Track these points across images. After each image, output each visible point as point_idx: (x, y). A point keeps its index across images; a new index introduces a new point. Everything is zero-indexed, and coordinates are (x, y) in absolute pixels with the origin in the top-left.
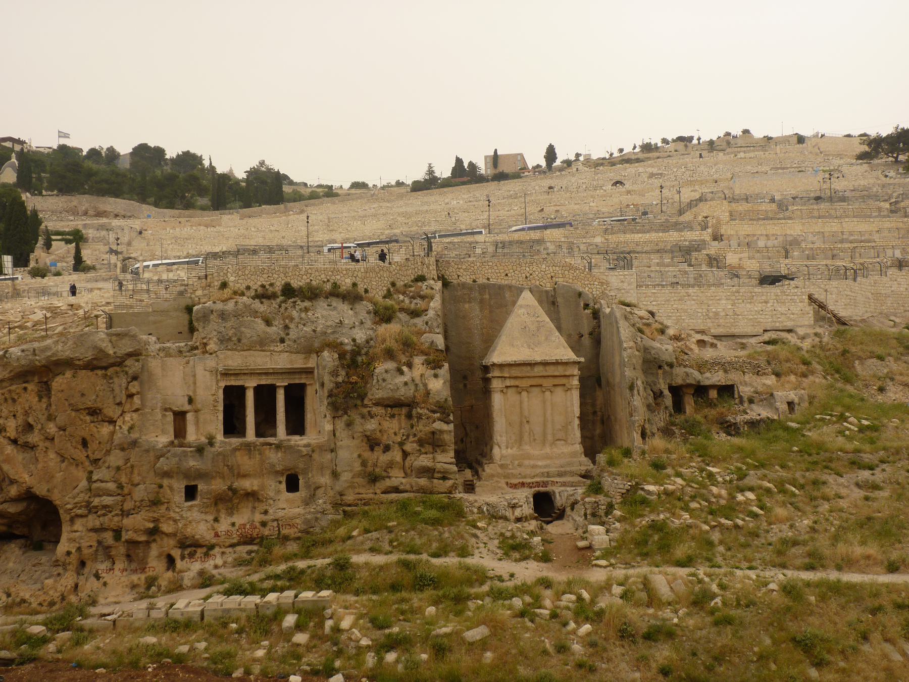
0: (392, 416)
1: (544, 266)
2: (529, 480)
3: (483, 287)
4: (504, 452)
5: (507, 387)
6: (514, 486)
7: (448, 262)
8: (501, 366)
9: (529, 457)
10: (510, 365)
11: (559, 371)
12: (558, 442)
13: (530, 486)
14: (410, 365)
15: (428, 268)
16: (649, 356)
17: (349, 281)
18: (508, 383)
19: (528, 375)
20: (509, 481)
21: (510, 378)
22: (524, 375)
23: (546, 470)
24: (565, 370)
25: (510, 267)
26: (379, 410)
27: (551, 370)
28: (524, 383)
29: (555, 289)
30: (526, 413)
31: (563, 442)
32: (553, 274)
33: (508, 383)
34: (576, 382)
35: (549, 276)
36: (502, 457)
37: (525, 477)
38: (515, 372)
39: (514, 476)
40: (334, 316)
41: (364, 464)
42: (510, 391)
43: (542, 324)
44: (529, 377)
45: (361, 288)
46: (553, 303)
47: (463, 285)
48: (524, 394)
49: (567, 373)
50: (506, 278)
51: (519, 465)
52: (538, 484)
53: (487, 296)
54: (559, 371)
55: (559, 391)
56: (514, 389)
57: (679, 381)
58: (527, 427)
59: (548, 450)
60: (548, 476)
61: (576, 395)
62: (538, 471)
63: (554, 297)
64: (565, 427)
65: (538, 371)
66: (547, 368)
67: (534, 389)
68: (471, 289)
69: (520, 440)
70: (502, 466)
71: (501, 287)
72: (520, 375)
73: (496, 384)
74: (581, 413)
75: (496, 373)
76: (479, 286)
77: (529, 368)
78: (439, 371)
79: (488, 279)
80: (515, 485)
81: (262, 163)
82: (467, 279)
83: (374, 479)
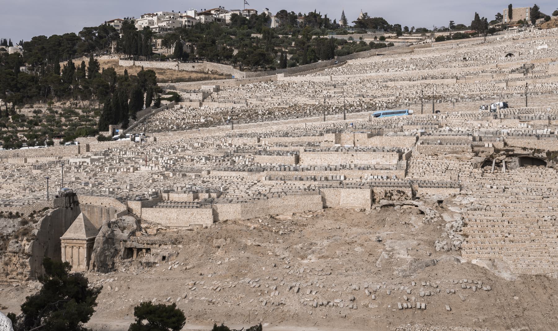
0: (15, 256)
3: (89, 206)
14: (22, 240)
17: (15, 211)
26: (11, 254)
38: (68, 241)
40: (5, 223)
41: (4, 270)
45: (20, 213)
57: (129, 246)
61: (85, 250)
65: (75, 241)
71: (94, 207)
78: (30, 243)
81: (365, 15)
83: (7, 274)
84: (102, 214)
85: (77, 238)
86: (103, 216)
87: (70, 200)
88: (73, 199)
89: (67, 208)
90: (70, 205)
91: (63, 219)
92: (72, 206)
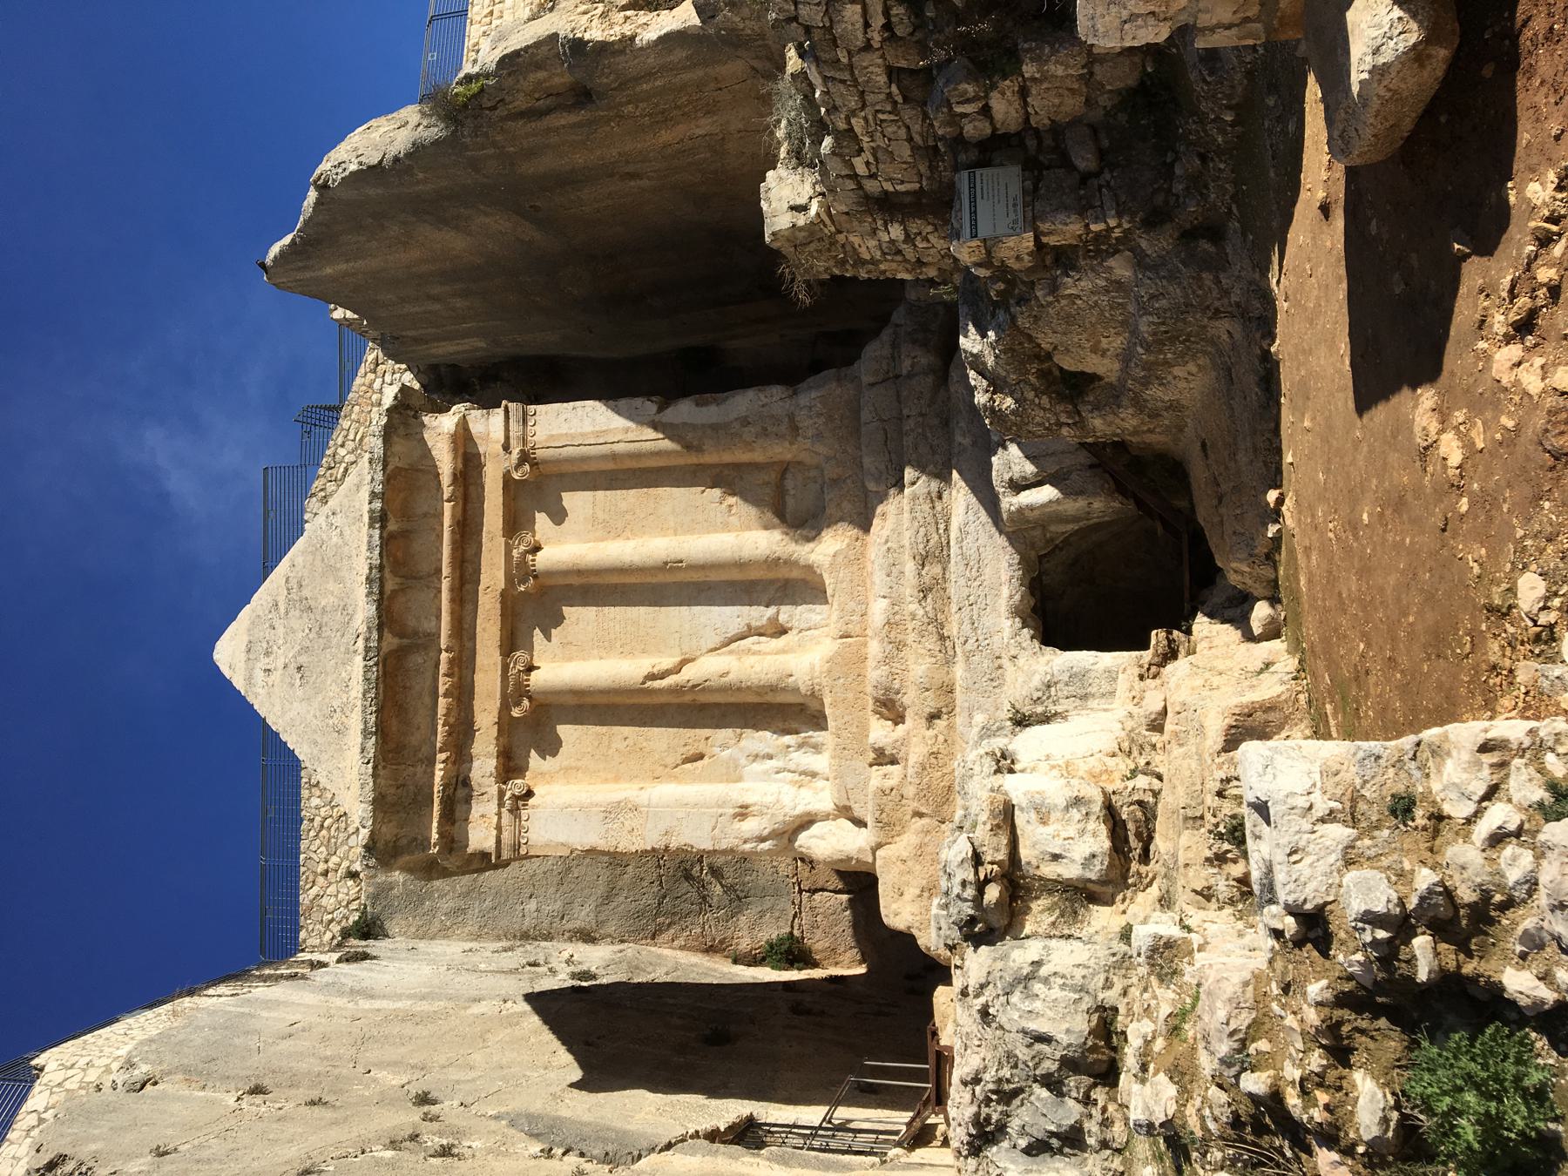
9: (849, 663)
18: (484, 765)
33: (484, 765)
49: (445, 463)
74: (648, 394)
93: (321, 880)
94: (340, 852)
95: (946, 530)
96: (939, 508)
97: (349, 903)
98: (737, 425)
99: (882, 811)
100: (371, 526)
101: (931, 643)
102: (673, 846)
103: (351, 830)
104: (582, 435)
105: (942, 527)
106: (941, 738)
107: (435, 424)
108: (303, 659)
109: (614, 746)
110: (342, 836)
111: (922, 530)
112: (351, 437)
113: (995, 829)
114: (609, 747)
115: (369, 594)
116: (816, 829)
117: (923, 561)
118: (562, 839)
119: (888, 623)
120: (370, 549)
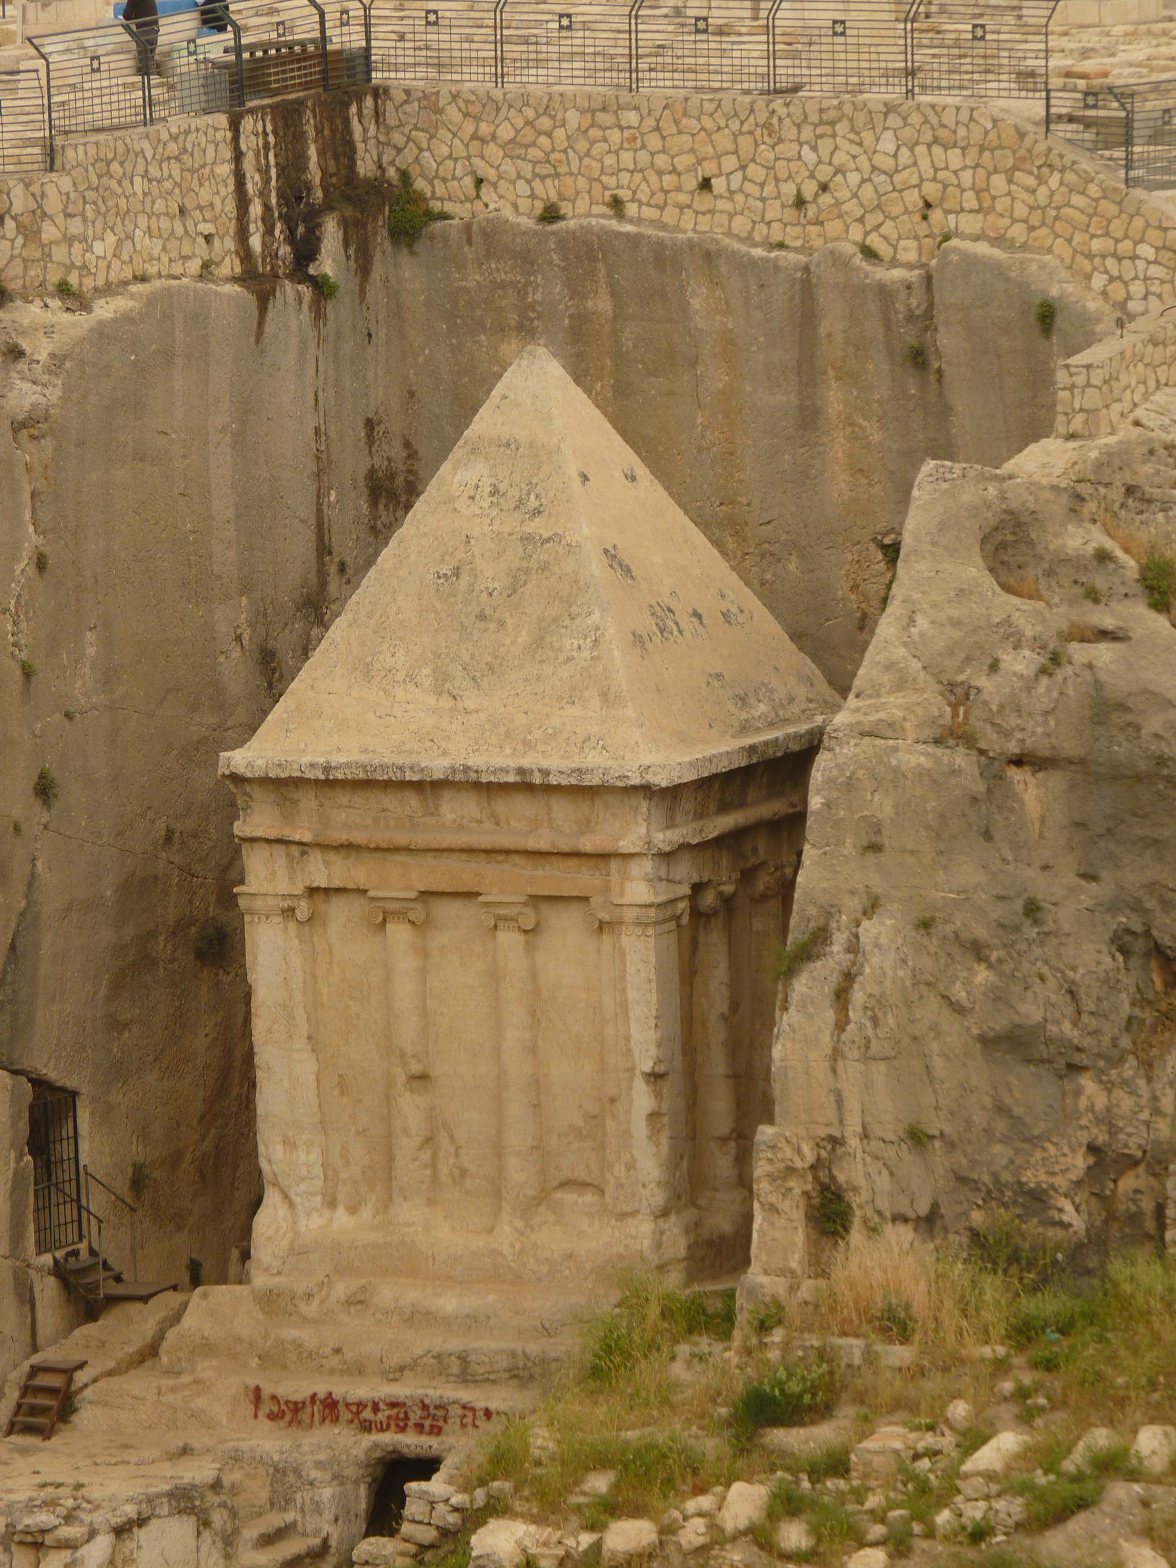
1: (888, 144)
2: (361, 1391)
3: (586, 253)
4: (313, 1223)
5: (312, 891)
6: (290, 1413)
7: (429, 102)
8: (284, 786)
10: (328, 784)
11: (559, 825)
12: (568, 1197)
13: (362, 1416)
15: (29, 233)
16: (1121, 750)
18: (319, 871)
19: (401, 838)
20: (267, 1389)
21: (324, 847)
22: (381, 837)
23: (455, 1344)
24: (586, 826)
25: (724, 141)
27: (519, 823)
28: (397, 880)
29: (929, 279)
30: (407, 1033)
31: (589, 1198)
32: (931, 190)
33: (319, 871)
34: (638, 888)
35: (913, 198)
36: (297, 1251)
37: (358, 1370)
38: (350, 818)
39: (308, 1358)
42: (339, 912)
43: (542, 555)
44: (407, 850)
46: (918, 358)
47: (489, 237)
48: (399, 932)
49: (587, 844)
50: (703, 202)
51: (358, 1301)
52: (399, 1415)
53: (602, 304)
54: (559, 825)
55: (566, 926)
56: (357, 905)
58: (411, 1109)
59: (506, 1236)
60: (466, 1377)
62: (423, 1343)
63: (926, 319)
64: (596, 1125)
66: (501, 806)
67: (446, 910)
68: (526, 259)
69: (383, 1177)
70: (268, 1300)
71: (665, 257)
72: (359, 837)
73: (265, 878)
75: (259, 820)
76: (565, 243)
77: (413, 800)
79: (617, 204)
80: (297, 1407)
82: (511, 205)
84: (808, 372)
85: (496, 759)
86: (834, 399)
87: (291, 167)
88: (341, 148)
89: (258, 281)
90: (306, 252)
91: (221, 466)
92: (330, 262)
93: (469, 127)
94: (508, 167)
95: (488, 1380)
96: (506, 1375)
97: (444, 180)
98: (626, 1157)
99: (278, 1295)
100: (521, 771)
101: (395, 1360)
102: (259, 1074)
103: (537, 185)
104: (624, 990)
105: (492, 1377)
106: (324, 1362)
107: (640, 820)
108: (465, 578)
109: (351, 1003)
110: (527, 169)
111: (486, 1360)
112: (1078, 200)
113: (58, 1540)
114: (351, 998)
115: (454, 770)
116: (283, 1211)
117: (463, 1358)
118: (261, 959)
119: (429, 1313)
120: (494, 772)
